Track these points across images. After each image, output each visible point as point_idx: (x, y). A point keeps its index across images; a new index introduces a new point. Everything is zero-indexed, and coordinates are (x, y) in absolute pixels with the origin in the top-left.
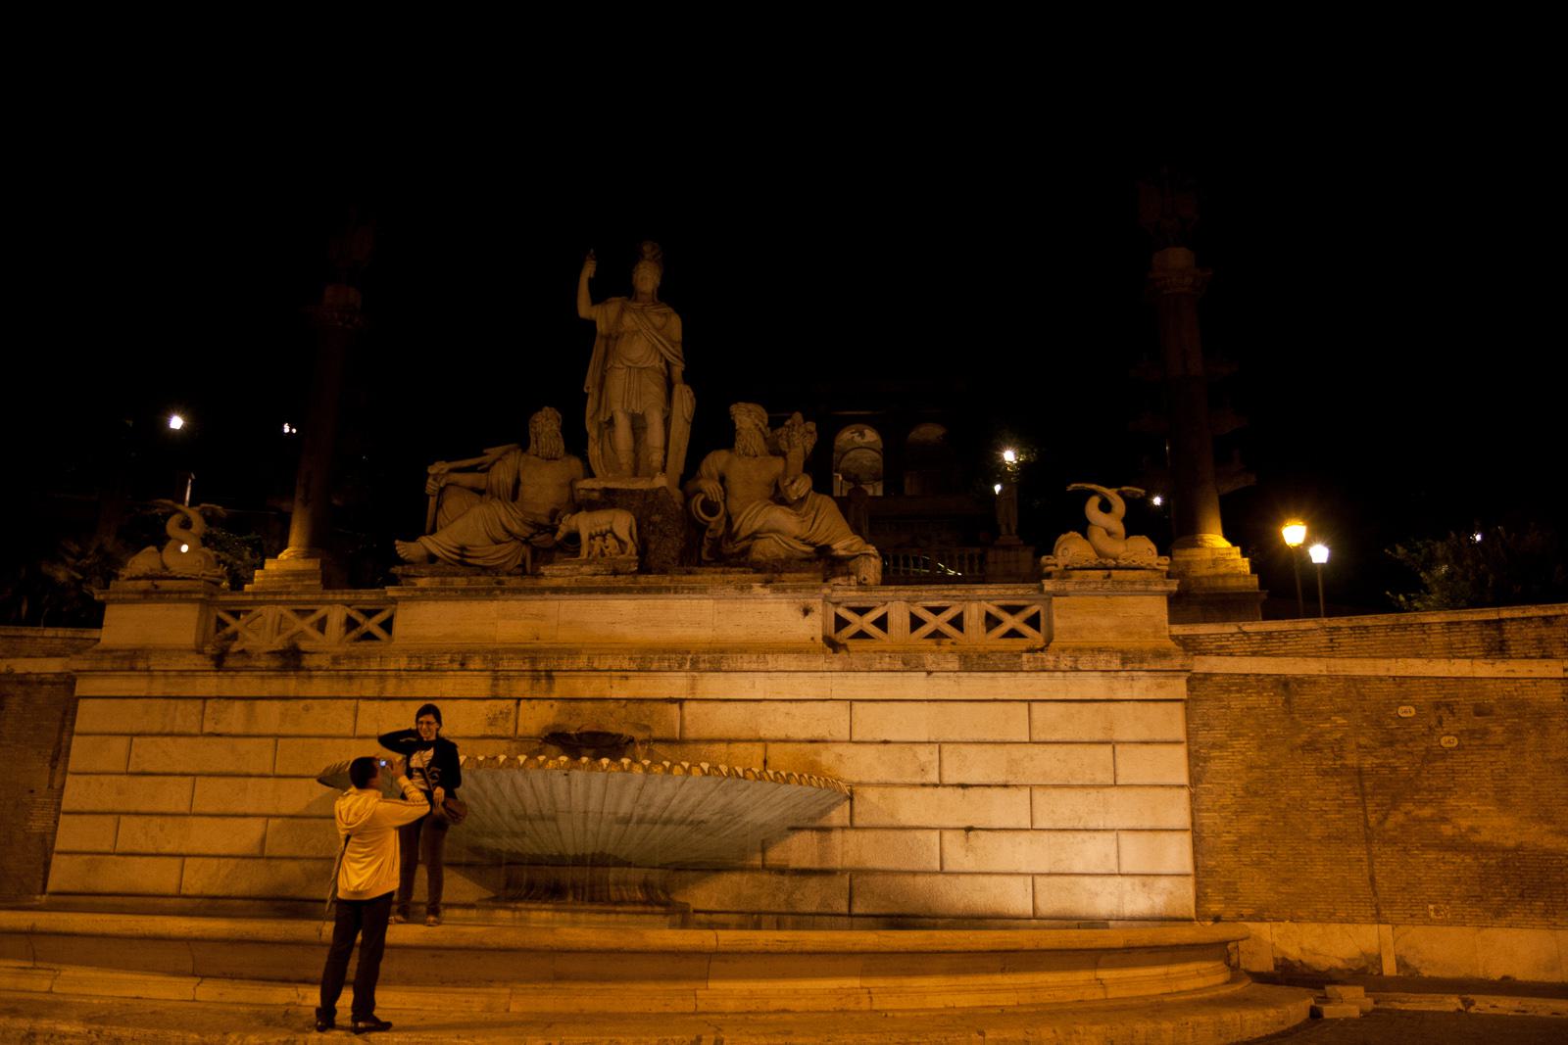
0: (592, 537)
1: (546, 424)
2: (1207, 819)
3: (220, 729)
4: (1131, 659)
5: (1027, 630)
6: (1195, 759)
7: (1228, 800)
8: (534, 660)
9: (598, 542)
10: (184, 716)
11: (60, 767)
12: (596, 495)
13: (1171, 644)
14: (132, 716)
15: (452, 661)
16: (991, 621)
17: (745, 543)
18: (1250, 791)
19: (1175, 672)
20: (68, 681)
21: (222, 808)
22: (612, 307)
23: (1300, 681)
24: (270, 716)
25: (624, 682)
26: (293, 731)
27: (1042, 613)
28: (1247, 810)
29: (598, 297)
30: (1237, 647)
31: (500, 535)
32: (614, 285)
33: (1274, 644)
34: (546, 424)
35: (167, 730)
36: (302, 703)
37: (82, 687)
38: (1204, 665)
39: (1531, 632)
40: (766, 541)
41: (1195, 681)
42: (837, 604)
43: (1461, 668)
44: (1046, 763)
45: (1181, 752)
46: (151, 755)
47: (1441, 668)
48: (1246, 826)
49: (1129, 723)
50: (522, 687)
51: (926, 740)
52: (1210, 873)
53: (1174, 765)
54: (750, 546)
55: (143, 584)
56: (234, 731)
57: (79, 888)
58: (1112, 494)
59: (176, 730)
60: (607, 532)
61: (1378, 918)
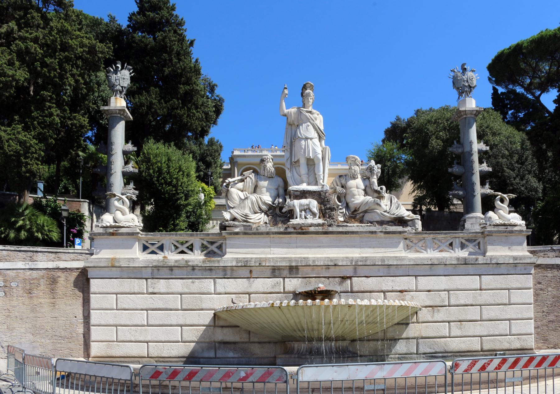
0: (301, 211)
3: (155, 291)
9: (303, 213)
12: (299, 193)
15: (255, 262)
17: (361, 215)
24: (177, 285)
25: (327, 270)
27: (481, 242)
31: (257, 209)
35: (132, 291)
36: (191, 280)
40: (373, 214)
42: (406, 239)
54: (363, 216)
56: (162, 291)
57: (105, 355)
59: (136, 291)
60: (307, 209)
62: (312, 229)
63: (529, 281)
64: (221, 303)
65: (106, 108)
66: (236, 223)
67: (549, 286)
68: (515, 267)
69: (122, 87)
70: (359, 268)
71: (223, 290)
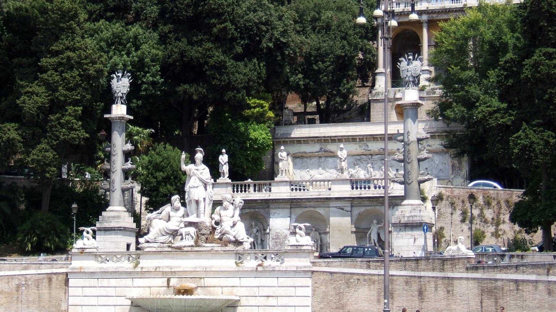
1: (175, 198)
6: (314, 291)
7: (318, 300)
8: (171, 268)
11: (67, 295)
21: (105, 304)
22: (191, 166)
24: (113, 282)
26: (118, 285)
28: (323, 302)
29: (186, 164)
30: (323, 264)
33: (330, 264)
34: (175, 198)
44: (280, 291)
46: (87, 291)
48: (322, 306)
51: (255, 285)
56: (106, 286)
58: (302, 225)
62: (185, 249)
63: (308, 282)
66: (147, 245)
68: (298, 273)
69: (122, 94)
70: (208, 273)
71: (136, 286)
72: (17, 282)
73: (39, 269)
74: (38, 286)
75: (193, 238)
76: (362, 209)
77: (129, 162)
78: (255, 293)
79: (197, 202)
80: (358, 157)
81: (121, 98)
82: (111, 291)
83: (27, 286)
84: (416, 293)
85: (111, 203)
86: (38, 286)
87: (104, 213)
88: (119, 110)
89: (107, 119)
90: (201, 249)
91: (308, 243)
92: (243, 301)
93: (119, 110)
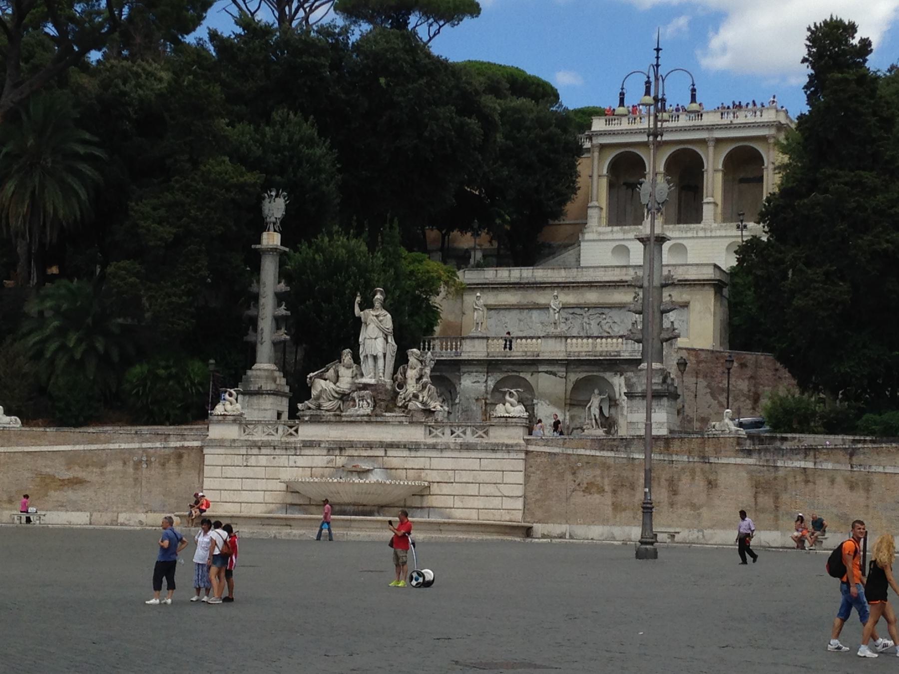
2: (530, 494)
4: (508, 448)
5: (484, 436)
6: (527, 477)
10: (238, 460)
13: (522, 442)
14: (220, 460)
16: (473, 433)
18: (540, 486)
19: (521, 451)
20: (201, 449)
23: (555, 454)
24: (263, 460)
32: (367, 304)
37: (206, 451)
38: (531, 448)
39: (610, 443)
41: (527, 453)
43: (593, 453)
45: (522, 474)
46: (229, 472)
47: (588, 452)
48: (538, 497)
49: (507, 465)
50: (337, 452)
52: (528, 510)
53: (520, 477)
55: (220, 418)
61: (567, 522)
64: (288, 475)
65: (258, 246)
67: (538, 470)
72: (135, 459)
73: (166, 441)
74: (163, 465)
75: (368, 403)
76: (582, 375)
77: (283, 307)
78: (450, 478)
79: (375, 358)
80: (571, 311)
81: (274, 224)
82: (260, 472)
83: (149, 463)
84: (666, 484)
85: (258, 359)
86: (163, 465)
87: (249, 373)
88: (272, 239)
89: (256, 249)
90: (379, 419)
91: (522, 415)
92: (435, 489)
93: (272, 239)
